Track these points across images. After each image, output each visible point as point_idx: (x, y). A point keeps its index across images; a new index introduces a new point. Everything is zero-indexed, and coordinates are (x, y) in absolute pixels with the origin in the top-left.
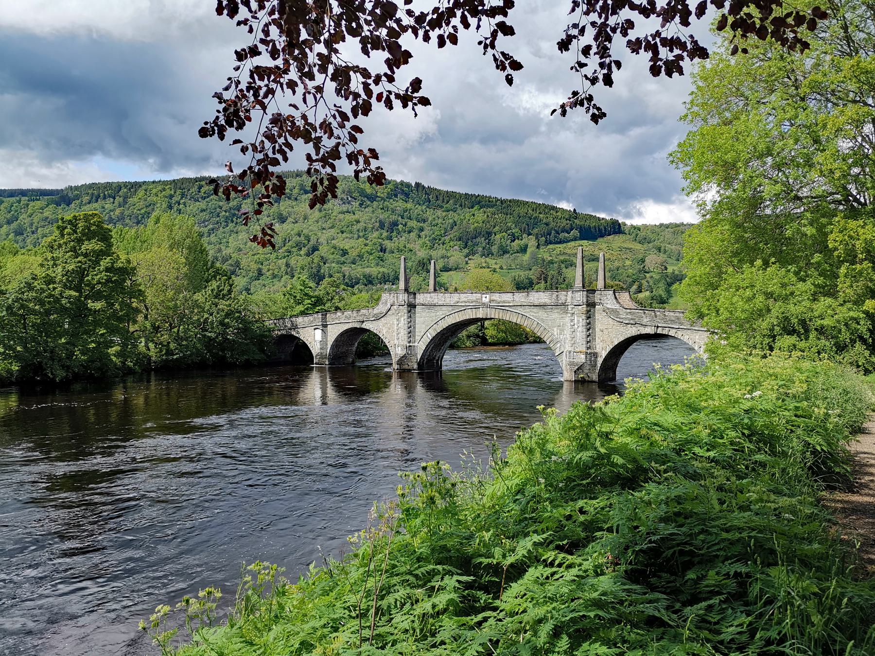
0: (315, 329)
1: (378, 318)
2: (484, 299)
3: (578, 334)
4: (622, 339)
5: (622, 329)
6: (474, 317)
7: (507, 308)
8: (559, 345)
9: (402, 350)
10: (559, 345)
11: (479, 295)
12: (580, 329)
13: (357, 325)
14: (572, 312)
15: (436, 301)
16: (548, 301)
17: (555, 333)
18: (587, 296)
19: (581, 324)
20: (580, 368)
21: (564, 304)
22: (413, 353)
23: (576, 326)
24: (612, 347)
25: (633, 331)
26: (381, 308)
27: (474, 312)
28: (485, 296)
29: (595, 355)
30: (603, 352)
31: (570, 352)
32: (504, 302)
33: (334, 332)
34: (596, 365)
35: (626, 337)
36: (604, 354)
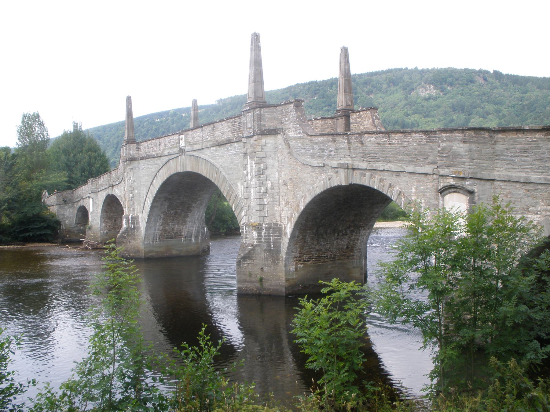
3: (252, 191)
4: (309, 199)
5: (306, 174)
16: (228, 135)
18: (260, 118)
23: (249, 177)
29: (276, 229)
34: (278, 251)
36: (289, 229)
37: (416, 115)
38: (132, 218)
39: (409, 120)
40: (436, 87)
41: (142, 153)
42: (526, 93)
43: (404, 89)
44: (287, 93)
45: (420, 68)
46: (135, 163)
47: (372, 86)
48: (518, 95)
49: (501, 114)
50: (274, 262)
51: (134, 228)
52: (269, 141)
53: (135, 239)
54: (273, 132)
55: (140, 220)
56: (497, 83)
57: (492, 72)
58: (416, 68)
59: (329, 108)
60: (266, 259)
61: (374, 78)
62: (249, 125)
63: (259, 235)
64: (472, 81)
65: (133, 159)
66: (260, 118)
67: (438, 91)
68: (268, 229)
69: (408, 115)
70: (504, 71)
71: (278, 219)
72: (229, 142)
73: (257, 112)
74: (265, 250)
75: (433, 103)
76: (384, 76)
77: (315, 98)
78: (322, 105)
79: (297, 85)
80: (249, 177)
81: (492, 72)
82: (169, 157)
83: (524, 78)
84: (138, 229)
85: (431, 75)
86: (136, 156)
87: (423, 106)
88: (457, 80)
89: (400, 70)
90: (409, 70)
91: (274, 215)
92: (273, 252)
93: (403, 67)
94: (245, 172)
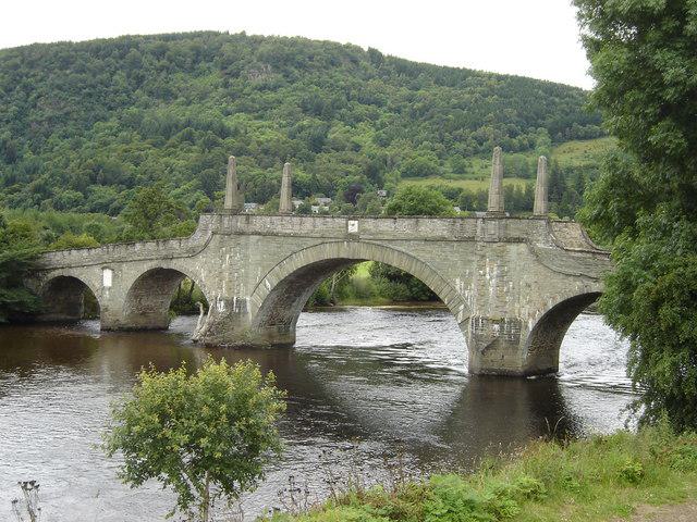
0: (103, 269)
1: (193, 253)
2: (350, 227)
4: (559, 300)
5: (558, 281)
6: (336, 257)
7: (385, 244)
9: (226, 306)
11: (343, 221)
14: (482, 253)
15: (279, 229)
17: (457, 287)
20: (493, 345)
21: (472, 239)
23: (488, 277)
24: (543, 313)
25: (576, 288)
26: (198, 239)
27: (336, 247)
28: (352, 222)
29: (517, 324)
33: (132, 273)
35: (566, 297)
36: (531, 326)
37: (243, 115)
39: (230, 123)
40: (276, 68)
41: (251, 228)
42: (418, 89)
43: (223, 68)
44: (16, 57)
45: (249, 34)
46: (243, 239)
47: (168, 59)
48: (405, 91)
49: (378, 122)
51: (239, 313)
52: (513, 248)
53: (239, 326)
54: (518, 241)
55: (248, 304)
56: (372, 70)
57: (366, 49)
58: (243, 33)
59: (93, 90)
60: (507, 349)
62: (493, 232)
63: (502, 328)
64: (333, 63)
65: (241, 233)
66: (506, 227)
67: (280, 76)
68: (510, 323)
69: (228, 114)
70: (385, 52)
72: (443, 239)
73: (504, 222)
75: (271, 96)
76: (190, 43)
77: (68, 72)
78: (80, 85)
79: (35, 46)
80: (488, 277)
81: (366, 49)
82: (320, 241)
83: (415, 64)
84: (246, 313)
85: (269, 47)
86: (246, 230)
87: (253, 100)
88: (311, 58)
89: (216, 34)
90: (232, 36)
91: (513, 311)
92: (514, 342)
93: (222, 31)
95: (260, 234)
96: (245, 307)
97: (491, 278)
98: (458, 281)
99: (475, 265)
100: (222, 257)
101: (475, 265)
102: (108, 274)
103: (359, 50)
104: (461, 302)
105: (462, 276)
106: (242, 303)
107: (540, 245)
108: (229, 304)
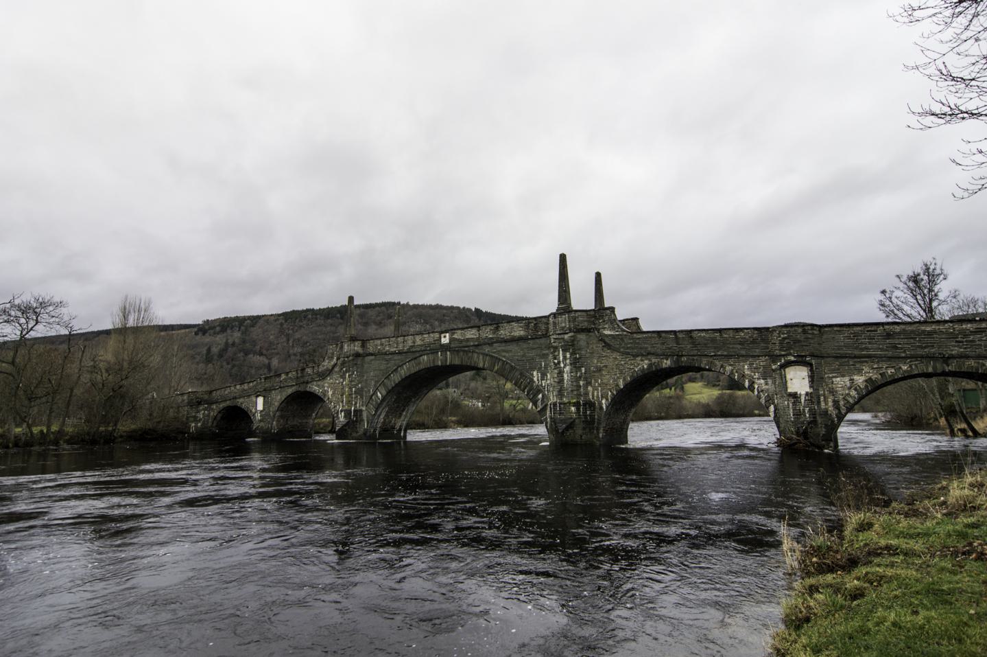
0: (257, 396)
1: (323, 376)
2: (443, 340)
3: (565, 376)
6: (432, 365)
8: (540, 396)
9: (345, 417)
10: (540, 396)
11: (437, 335)
12: (567, 369)
13: (301, 389)
17: (535, 379)
19: (568, 361)
22: (359, 419)
23: (562, 365)
28: (443, 335)
30: (604, 401)
31: (555, 404)
32: (468, 340)
38: (354, 411)
50: (590, 430)
51: (356, 421)
61: (370, 312)
62: (563, 325)
63: (578, 409)
68: (584, 405)
71: (591, 397)
74: (583, 421)
80: (562, 365)
84: (362, 420)
94: (556, 361)
95: (372, 354)
96: (361, 415)
97: (565, 366)
98: (535, 373)
99: (551, 357)
100: (343, 377)
101: (551, 357)
102: (260, 401)
103: (469, 310)
104: (539, 391)
105: (539, 370)
106: (358, 412)
107: (607, 332)
108: (348, 413)
